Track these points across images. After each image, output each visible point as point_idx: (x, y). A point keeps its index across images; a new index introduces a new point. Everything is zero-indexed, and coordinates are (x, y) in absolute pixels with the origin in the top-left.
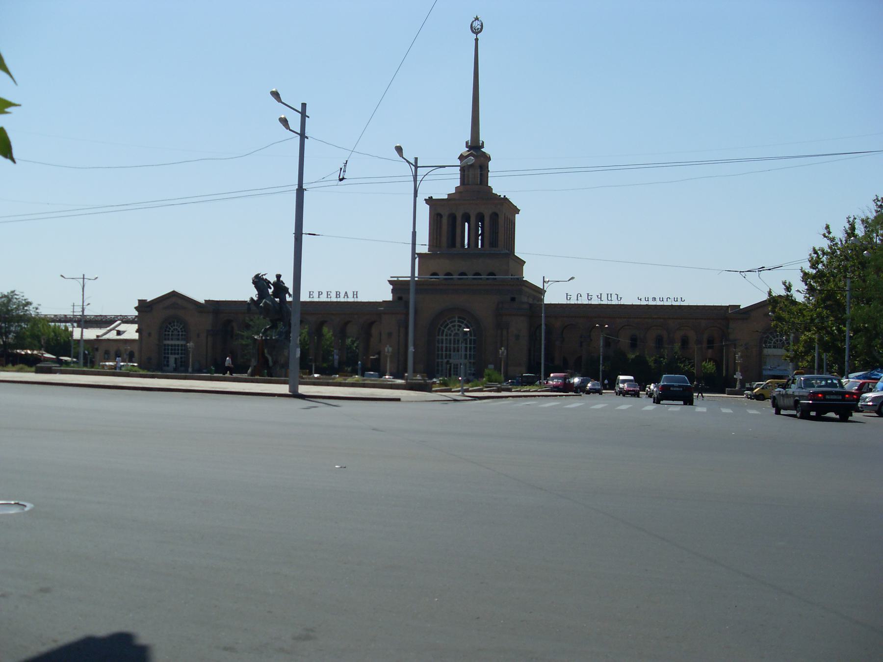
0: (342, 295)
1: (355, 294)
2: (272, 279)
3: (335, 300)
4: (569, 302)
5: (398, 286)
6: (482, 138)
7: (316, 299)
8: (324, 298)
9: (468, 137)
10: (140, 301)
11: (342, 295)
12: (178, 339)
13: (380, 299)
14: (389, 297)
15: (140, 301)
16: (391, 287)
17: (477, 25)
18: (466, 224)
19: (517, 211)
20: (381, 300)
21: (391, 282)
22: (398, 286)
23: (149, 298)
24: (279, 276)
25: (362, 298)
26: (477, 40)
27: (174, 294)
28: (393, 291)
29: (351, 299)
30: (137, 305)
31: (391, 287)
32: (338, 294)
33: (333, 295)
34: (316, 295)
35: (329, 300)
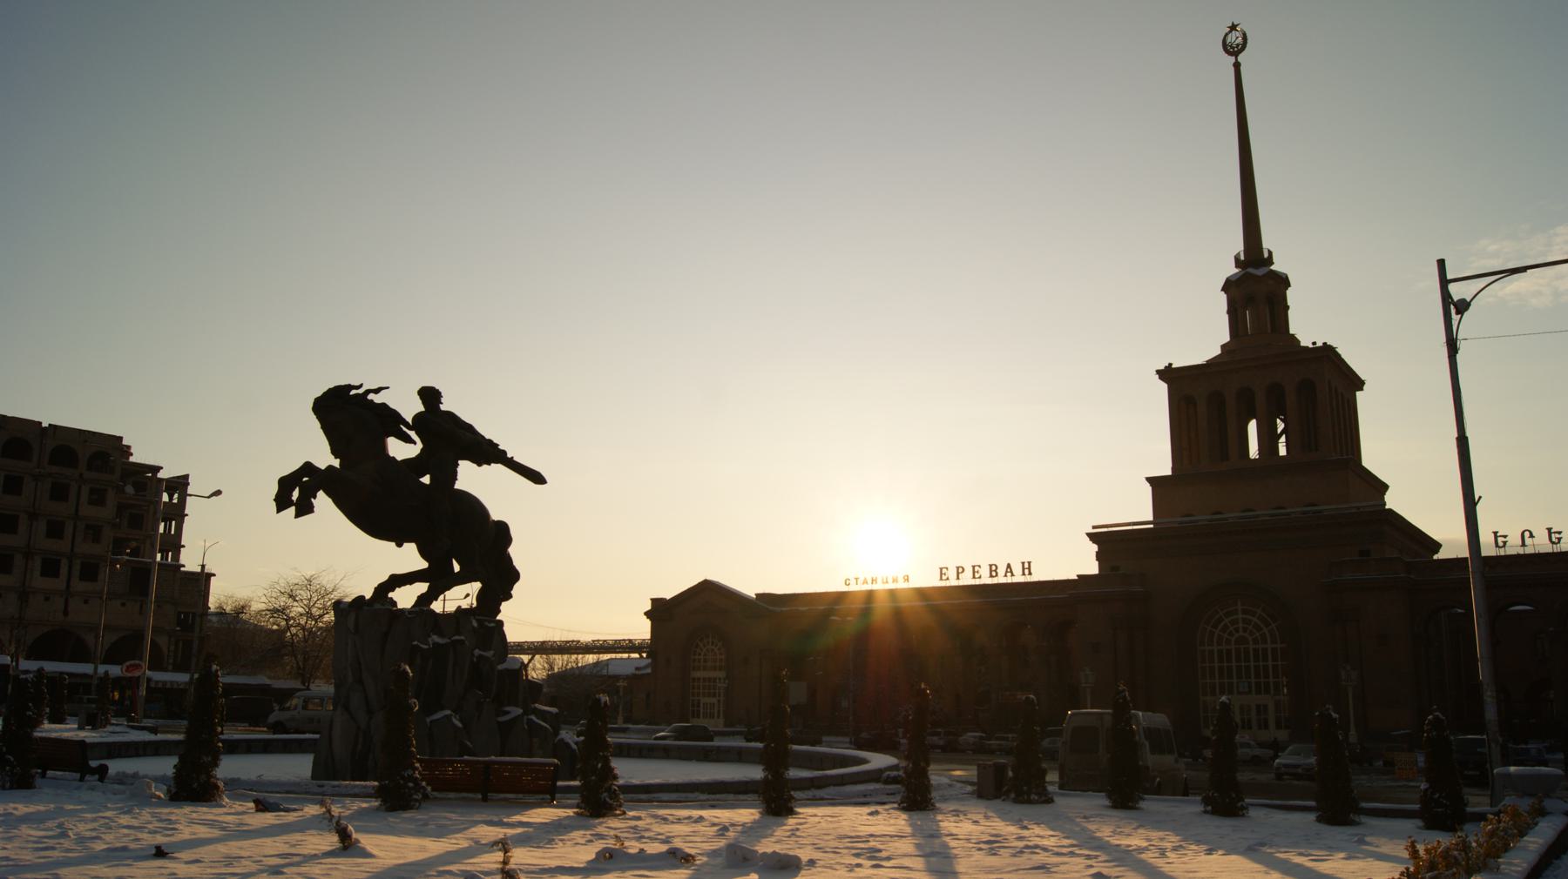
0: (1001, 571)
1: (1027, 568)
2: (410, 408)
3: (989, 581)
4: (1502, 552)
5: (1107, 541)
6: (1268, 242)
7: (953, 582)
8: (967, 580)
9: (1237, 245)
10: (653, 600)
11: (1001, 571)
12: (715, 669)
13: (1069, 573)
14: (1092, 568)
15: (653, 600)
16: (1095, 548)
17: (1232, 38)
18: (1252, 427)
19: (1359, 384)
20: (1072, 575)
21: (1093, 537)
22: (1107, 541)
23: (668, 596)
24: (430, 395)
25: (1040, 574)
26: (1237, 66)
27: (707, 590)
28: (1099, 556)
29: (1019, 578)
30: (648, 607)
31: (1095, 548)
32: (993, 570)
33: (985, 572)
34: (952, 573)
35: (978, 582)
